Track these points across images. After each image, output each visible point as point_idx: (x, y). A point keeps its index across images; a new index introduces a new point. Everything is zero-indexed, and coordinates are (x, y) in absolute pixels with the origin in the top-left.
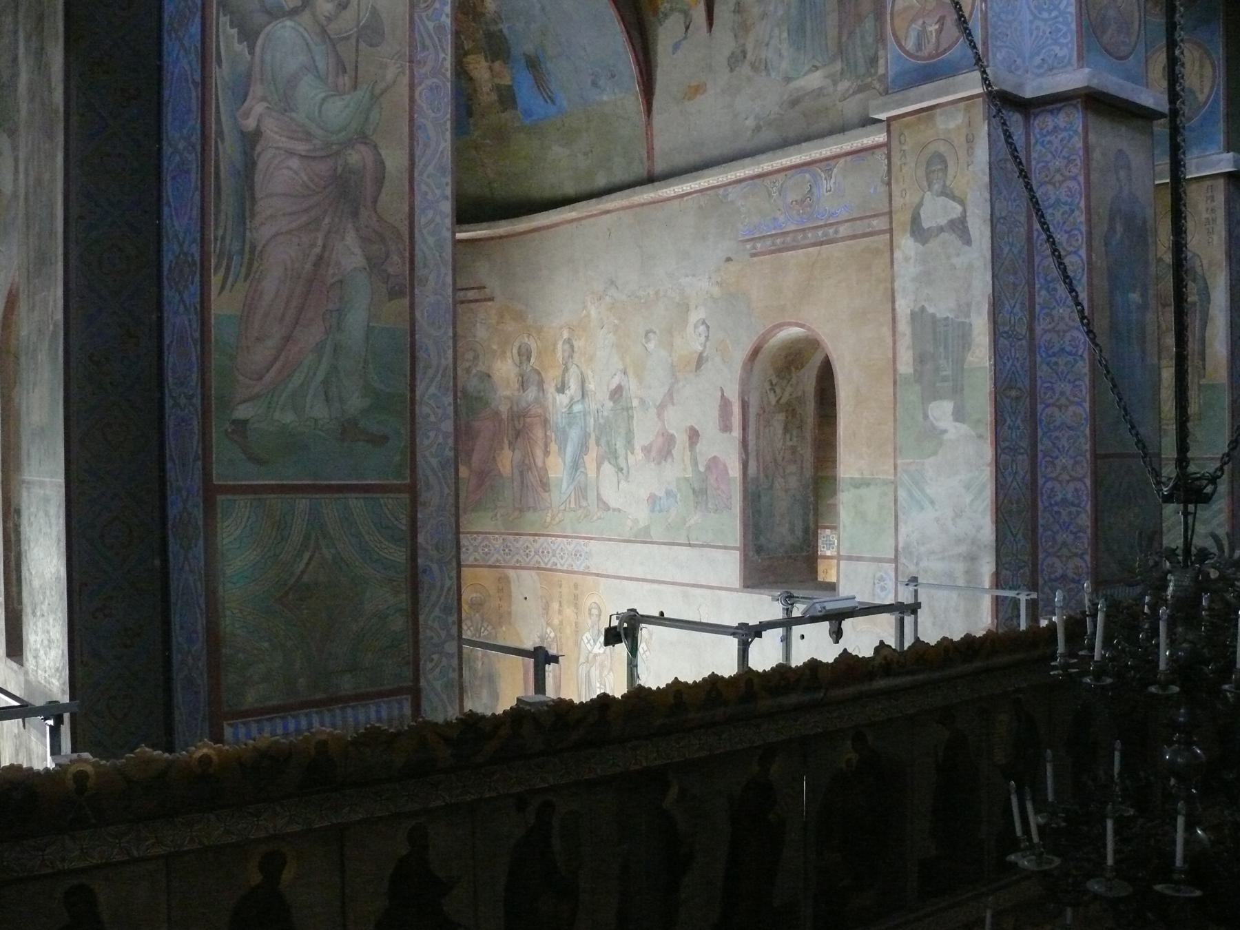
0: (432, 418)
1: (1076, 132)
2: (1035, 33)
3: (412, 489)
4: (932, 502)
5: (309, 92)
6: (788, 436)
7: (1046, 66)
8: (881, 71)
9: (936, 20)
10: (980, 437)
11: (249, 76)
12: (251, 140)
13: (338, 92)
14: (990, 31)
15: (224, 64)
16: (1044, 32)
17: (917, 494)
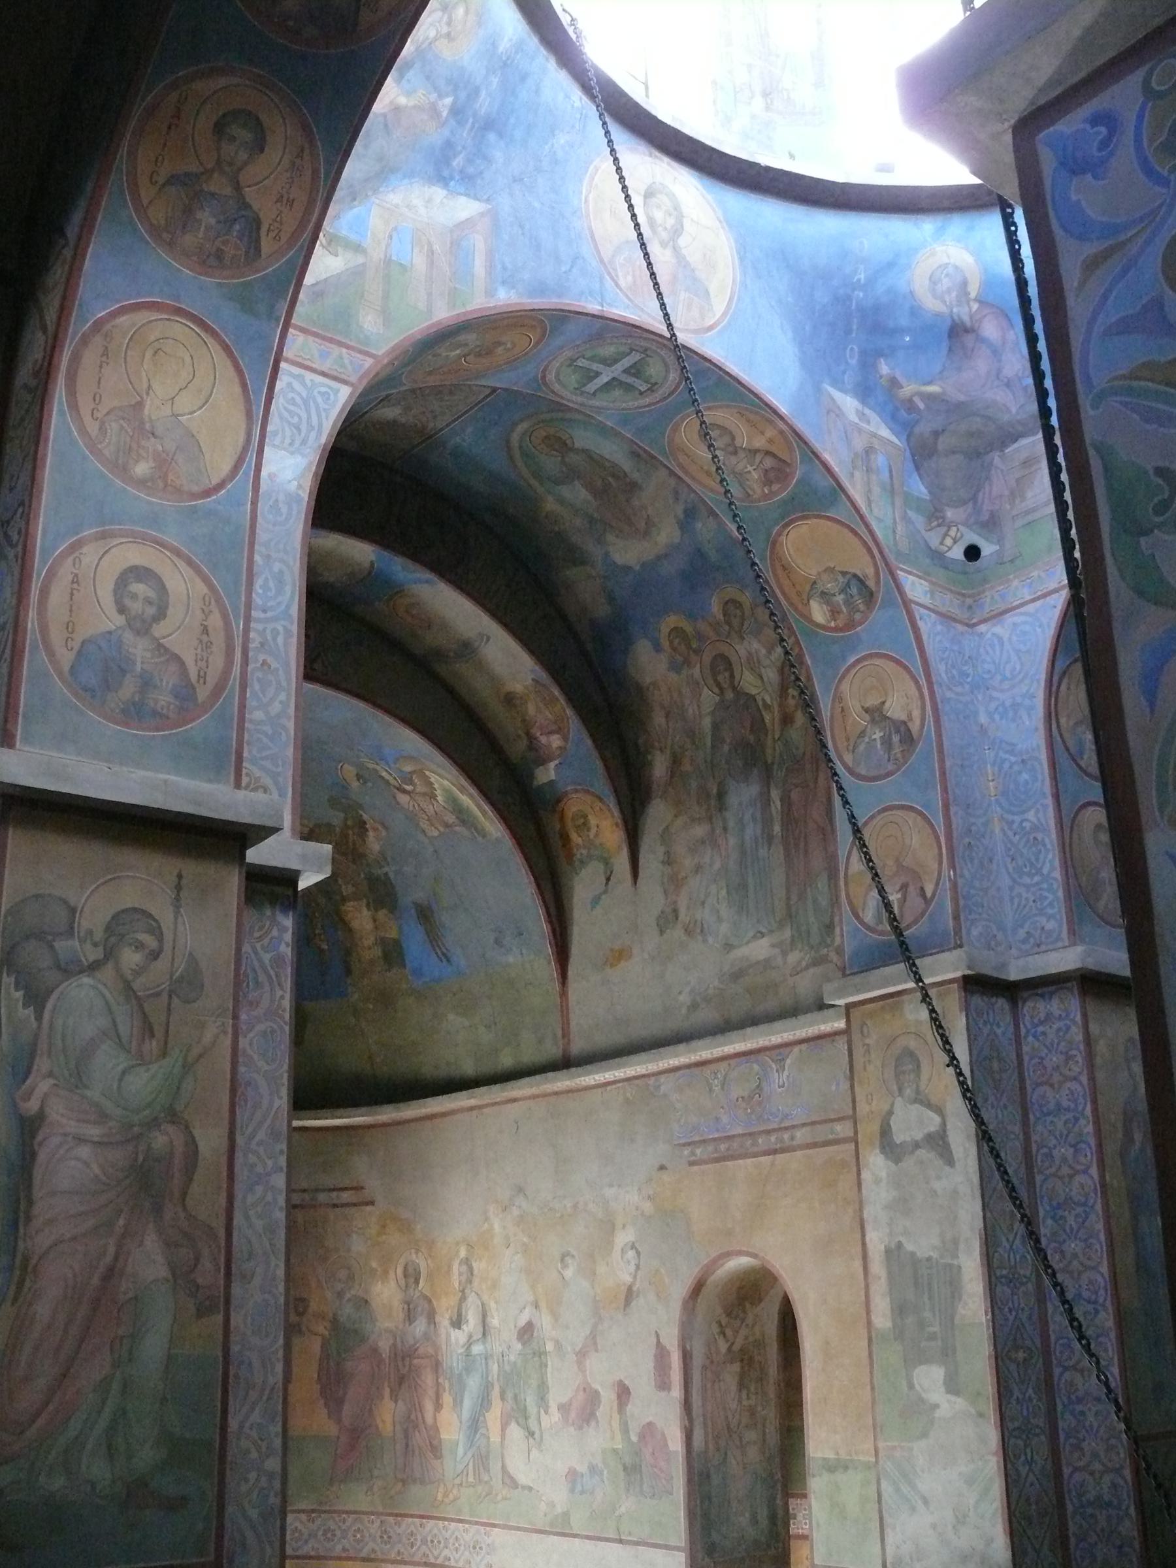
0: (254, 1455)
1: (1074, 1021)
2: (1016, 901)
4: (926, 1502)
6: (744, 1393)
7: (1032, 940)
8: (838, 941)
9: (897, 887)
10: (981, 1415)
11: (34, 1045)
13: (142, 1060)
14: (962, 902)
16: (1027, 899)
17: (905, 1489)
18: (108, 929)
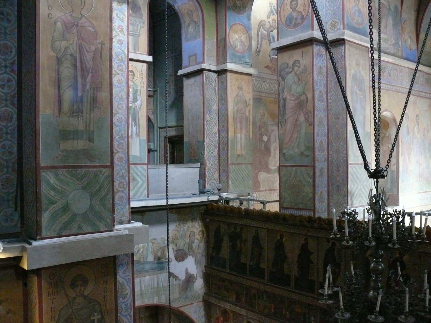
0: (341, 150)
3: (314, 167)
5: (294, 87)
12: (285, 100)
13: (299, 85)
18: (293, 65)
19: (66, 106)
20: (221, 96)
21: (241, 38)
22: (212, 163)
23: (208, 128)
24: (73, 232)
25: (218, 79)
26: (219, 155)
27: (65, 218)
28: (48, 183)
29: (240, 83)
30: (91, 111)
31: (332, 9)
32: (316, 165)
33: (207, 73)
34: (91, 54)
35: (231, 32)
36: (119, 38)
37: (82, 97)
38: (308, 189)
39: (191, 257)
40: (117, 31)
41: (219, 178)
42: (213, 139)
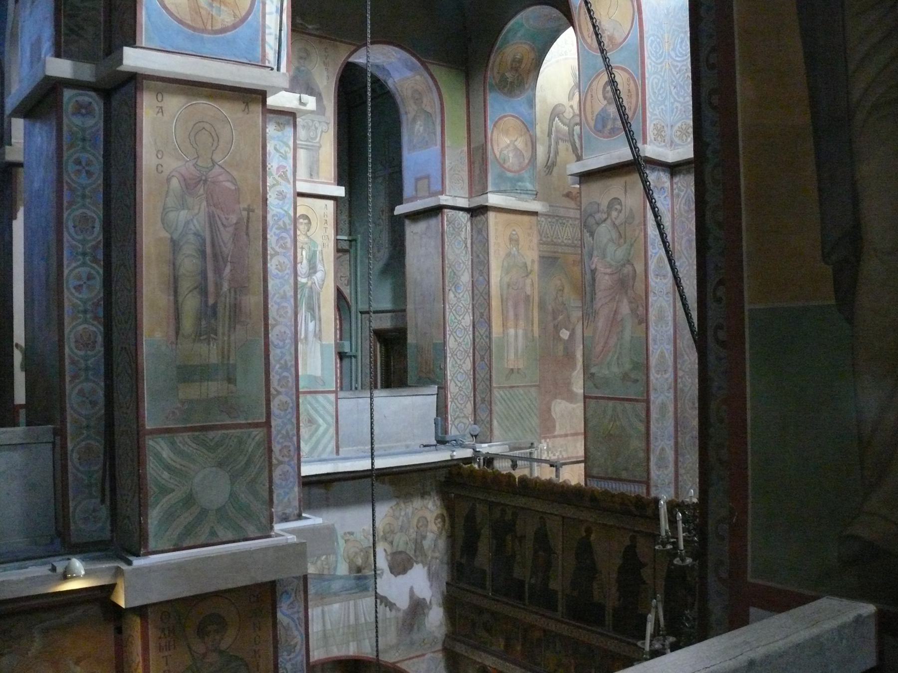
3: (648, 401)
5: (611, 248)
11: (593, 249)
12: (593, 272)
13: (619, 246)
15: (586, 248)
18: (608, 207)
19: (188, 324)
20: (478, 256)
21: (516, 143)
22: (459, 384)
23: (451, 319)
24: (202, 539)
25: (472, 224)
26: (474, 371)
27: (186, 518)
28: (158, 456)
29: (514, 230)
30: (232, 329)
31: (681, 99)
32: (652, 398)
33: (450, 214)
34: (231, 229)
35: (495, 133)
36: (278, 188)
37: (215, 306)
38: (637, 444)
39: (420, 565)
40: (276, 177)
41: (475, 415)
42: (462, 339)
